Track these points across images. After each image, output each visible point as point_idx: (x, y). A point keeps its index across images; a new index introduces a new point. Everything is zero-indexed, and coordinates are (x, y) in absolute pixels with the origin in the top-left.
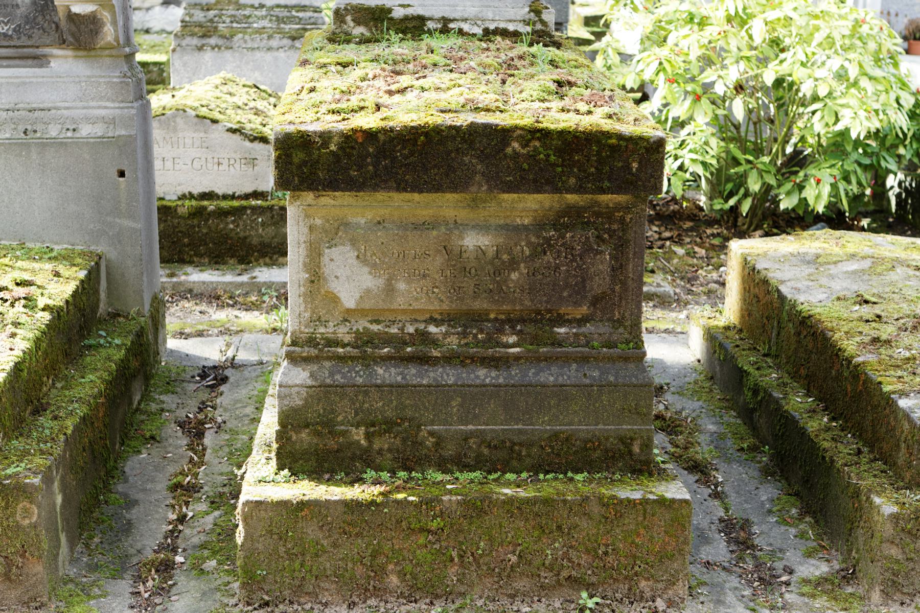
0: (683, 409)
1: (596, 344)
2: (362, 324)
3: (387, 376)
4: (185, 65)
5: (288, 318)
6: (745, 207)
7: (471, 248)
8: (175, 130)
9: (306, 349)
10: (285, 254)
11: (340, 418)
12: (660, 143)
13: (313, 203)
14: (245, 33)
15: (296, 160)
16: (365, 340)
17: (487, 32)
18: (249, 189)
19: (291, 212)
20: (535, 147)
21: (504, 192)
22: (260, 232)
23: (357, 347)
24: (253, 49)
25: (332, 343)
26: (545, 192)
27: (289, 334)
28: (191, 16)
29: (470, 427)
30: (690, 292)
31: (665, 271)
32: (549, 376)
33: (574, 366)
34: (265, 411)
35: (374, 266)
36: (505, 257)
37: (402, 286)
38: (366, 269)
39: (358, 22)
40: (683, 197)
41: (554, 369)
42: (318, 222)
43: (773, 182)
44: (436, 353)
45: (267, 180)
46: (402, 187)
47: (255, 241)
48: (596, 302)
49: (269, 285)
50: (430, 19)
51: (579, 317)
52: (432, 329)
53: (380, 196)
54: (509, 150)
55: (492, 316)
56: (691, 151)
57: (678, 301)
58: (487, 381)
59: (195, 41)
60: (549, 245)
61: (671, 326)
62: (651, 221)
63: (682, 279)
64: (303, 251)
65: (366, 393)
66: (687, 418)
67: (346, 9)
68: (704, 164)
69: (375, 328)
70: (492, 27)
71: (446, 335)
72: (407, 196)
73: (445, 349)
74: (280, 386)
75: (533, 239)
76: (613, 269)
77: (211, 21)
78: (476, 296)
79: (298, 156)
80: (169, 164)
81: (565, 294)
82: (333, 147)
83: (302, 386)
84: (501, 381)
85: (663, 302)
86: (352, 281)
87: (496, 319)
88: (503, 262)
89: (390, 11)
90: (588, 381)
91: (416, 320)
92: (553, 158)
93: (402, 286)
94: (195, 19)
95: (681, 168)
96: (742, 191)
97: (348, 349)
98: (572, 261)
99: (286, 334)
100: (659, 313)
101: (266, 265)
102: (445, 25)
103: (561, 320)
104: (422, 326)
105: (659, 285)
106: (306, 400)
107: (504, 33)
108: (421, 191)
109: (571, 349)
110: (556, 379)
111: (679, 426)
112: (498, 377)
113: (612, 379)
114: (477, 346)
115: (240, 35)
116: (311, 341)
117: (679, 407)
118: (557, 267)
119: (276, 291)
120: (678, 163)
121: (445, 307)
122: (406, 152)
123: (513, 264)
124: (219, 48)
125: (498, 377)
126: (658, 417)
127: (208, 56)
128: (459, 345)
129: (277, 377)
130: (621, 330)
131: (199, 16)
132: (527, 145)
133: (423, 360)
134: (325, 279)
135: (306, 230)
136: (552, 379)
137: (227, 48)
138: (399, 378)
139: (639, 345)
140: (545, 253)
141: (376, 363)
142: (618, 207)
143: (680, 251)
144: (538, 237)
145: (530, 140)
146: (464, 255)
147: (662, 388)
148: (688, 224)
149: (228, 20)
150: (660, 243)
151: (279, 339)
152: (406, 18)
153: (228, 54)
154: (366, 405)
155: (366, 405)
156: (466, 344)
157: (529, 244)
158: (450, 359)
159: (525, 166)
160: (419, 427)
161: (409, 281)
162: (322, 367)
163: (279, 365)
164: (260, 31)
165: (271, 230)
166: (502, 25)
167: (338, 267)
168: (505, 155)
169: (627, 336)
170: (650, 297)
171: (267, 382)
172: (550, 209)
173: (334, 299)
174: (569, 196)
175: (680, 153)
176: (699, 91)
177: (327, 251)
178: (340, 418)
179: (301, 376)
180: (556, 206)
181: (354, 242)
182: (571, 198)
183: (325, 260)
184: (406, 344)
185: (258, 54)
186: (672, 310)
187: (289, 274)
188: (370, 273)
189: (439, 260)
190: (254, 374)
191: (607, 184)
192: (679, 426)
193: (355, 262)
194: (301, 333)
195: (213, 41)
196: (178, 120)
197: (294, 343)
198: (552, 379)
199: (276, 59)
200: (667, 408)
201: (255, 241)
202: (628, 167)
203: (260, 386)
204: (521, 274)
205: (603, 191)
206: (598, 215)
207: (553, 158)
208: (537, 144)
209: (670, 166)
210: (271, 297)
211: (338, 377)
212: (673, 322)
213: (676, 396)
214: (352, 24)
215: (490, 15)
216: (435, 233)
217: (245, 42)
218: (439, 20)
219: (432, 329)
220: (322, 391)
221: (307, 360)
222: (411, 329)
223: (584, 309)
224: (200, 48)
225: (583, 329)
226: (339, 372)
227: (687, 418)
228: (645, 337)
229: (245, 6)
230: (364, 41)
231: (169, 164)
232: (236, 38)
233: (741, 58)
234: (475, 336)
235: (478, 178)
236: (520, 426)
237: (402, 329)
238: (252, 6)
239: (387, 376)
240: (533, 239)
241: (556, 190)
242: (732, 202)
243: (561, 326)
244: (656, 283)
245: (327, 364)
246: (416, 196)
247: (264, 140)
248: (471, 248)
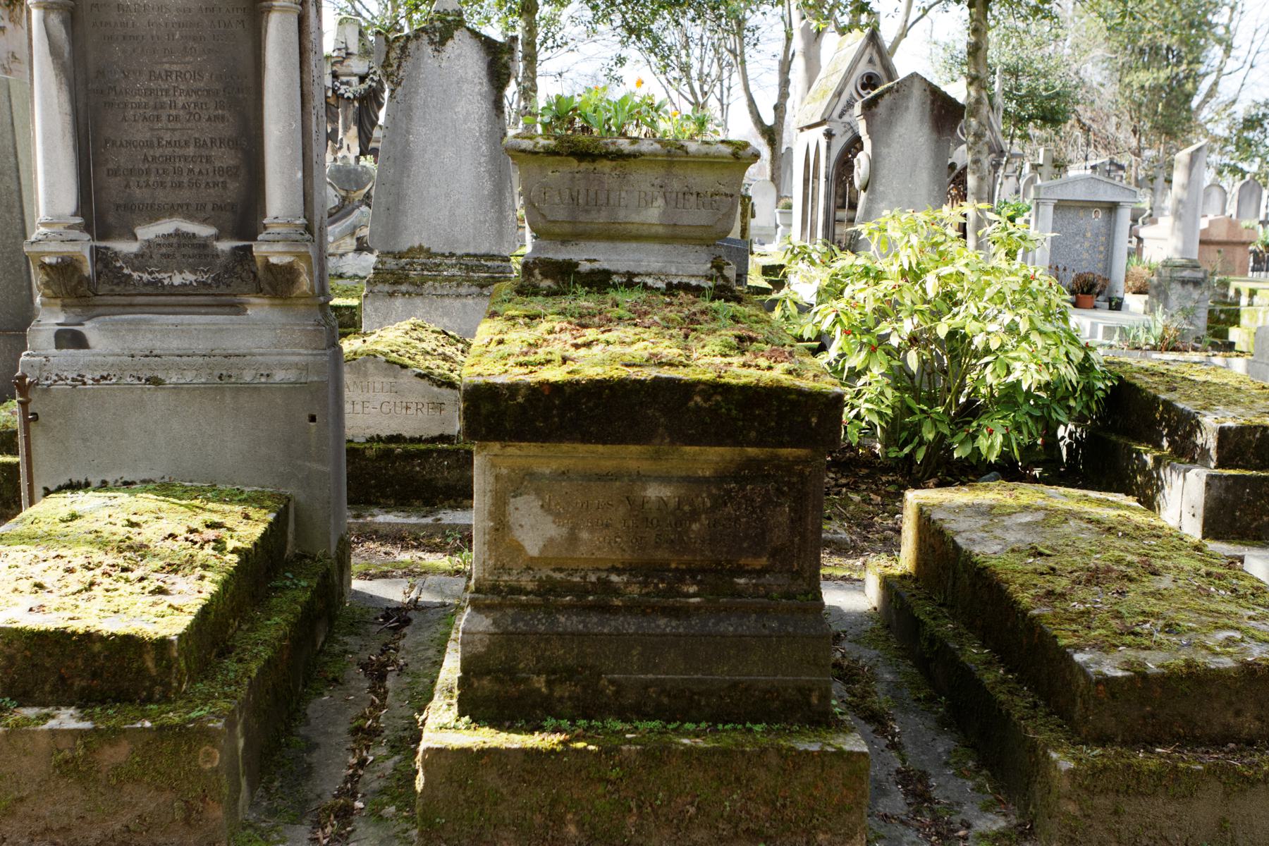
0: (860, 657)
1: (775, 595)
2: (545, 572)
3: (569, 623)
4: (376, 310)
5: (473, 561)
6: (920, 456)
7: (653, 498)
8: (366, 375)
9: (490, 596)
10: (472, 498)
11: (522, 665)
12: (839, 399)
13: (500, 453)
14: (435, 280)
15: (484, 411)
16: (548, 589)
17: (669, 285)
18: (436, 433)
19: (477, 461)
20: (717, 402)
21: (686, 445)
22: (446, 474)
23: (540, 595)
24: (442, 296)
25: (516, 590)
26: (726, 445)
27: (473, 581)
28: (383, 263)
29: (650, 676)
30: (866, 539)
31: (841, 517)
32: (728, 627)
33: (754, 616)
34: (447, 656)
35: (558, 515)
36: (687, 508)
37: (585, 535)
38: (550, 518)
39: (545, 275)
40: (859, 444)
41: (734, 619)
42: (504, 471)
43: (947, 431)
44: (617, 602)
45: (456, 426)
46: (586, 439)
47: (440, 484)
48: (774, 554)
49: (453, 527)
50: (616, 273)
51: (758, 567)
52: (614, 578)
53: (565, 447)
54: (692, 404)
55: (673, 566)
57: (854, 548)
58: (668, 630)
59: (387, 288)
60: (731, 498)
61: (847, 573)
62: (829, 466)
63: (858, 526)
64: (488, 500)
65: (548, 641)
66: (863, 667)
67: (534, 263)
69: (558, 576)
70: (675, 281)
71: (628, 583)
72: (591, 447)
73: (626, 598)
74: (463, 633)
75: (714, 491)
76: (792, 521)
77: (403, 268)
78: (657, 546)
79: (486, 408)
80: (358, 408)
81: (745, 545)
82: (520, 400)
83: (484, 633)
84: (681, 630)
85: (841, 549)
86: (535, 530)
87: (677, 569)
88: (685, 513)
89: (577, 265)
90: (767, 632)
91: (598, 569)
92: (734, 412)
93: (585, 535)
94: (387, 266)
95: (857, 416)
96: (916, 440)
97: (531, 596)
98: (752, 513)
99: (470, 578)
100: (836, 560)
101: (451, 507)
102: (630, 280)
103: (741, 572)
104: (604, 575)
105: (835, 532)
106: (488, 646)
107: (687, 288)
108: (604, 443)
109: (750, 600)
110: (736, 630)
111: (856, 674)
112: (678, 626)
113: (791, 630)
114: (658, 596)
115: (430, 283)
116: (495, 589)
117: (856, 655)
118: (737, 519)
119: (460, 533)
120: (854, 412)
121: (627, 556)
122: (591, 404)
123: (694, 515)
124: (410, 294)
125: (678, 626)
126: (836, 665)
127: (399, 302)
128: (640, 595)
129: (462, 621)
130: (800, 581)
131: (391, 263)
132: (709, 400)
133: (604, 609)
134: (510, 528)
135: (492, 479)
136: (731, 629)
137: (417, 295)
138: (581, 627)
139: (818, 596)
140: (726, 505)
141: (558, 611)
142: (798, 461)
143: (856, 498)
144: (719, 489)
145: (712, 395)
146: (646, 506)
147: (839, 635)
148: (864, 471)
149: (419, 268)
150: (836, 489)
151: (462, 582)
152: (592, 272)
153: (418, 301)
154: (548, 653)
155: (548, 653)
156: (647, 594)
157: (710, 495)
158: (630, 608)
159: (708, 420)
160: (599, 675)
161: (592, 531)
162: (505, 614)
163: (462, 608)
164: (449, 279)
165: (456, 474)
166: (685, 280)
167: (523, 516)
168: (688, 409)
169: (805, 587)
170: (828, 543)
171: (450, 625)
172: (732, 461)
173: (519, 548)
174: (749, 449)
175: (856, 402)
176: (874, 342)
177: (512, 500)
178: (522, 665)
179: (484, 623)
180: (737, 458)
181: (538, 492)
182: (752, 451)
183: (511, 508)
184: (589, 593)
185: (447, 301)
186: (849, 557)
187: (475, 517)
188: (554, 522)
189: (622, 510)
190: (436, 617)
191: (787, 438)
192: (856, 674)
193: (539, 511)
194: (485, 580)
195: (404, 288)
196: (369, 365)
197: (478, 590)
198: (731, 629)
199: (464, 306)
200: (843, 656)
201: (440, 484)
202: (808, 422)
203: (443, 630)
204: (702, 525)
205: (783, 445)
206: (778, 467)
207: (734, 412)
208: (719, 398)
209: (848, 415)
210: (455, 539)
211: (520, 624)
212: (850, 569)
213: (853, 645)
214: (540, 277)
215: (674, 270)
216: (618, 483)
217: (435, 289)
218: (623, 275)
219: (614, 578)
220: (504, 639)
221: (489, 608)
222: (593, 578)
223: (764, 561)
224: (391, 295)
225: (762, 580)
226: (522, 620)
227: (863, 667)
228: (823, 584)
229: (436, 255)
230: (551, 293)
231: (358, 408)
232: (426, 286)
233: (916, 311)
234: (656, 585)
235: (661, 430)
236: (700, 676)
237: (584, 578)
238: (443, 255)
239: (569, 623)
240: (714, 491)
241: (737, 443)
242: (906, 450)
243: (740, 577)
244: (835, 529)
245: (510, 611)
246: (600, 448)
247: (451, 385)
248: (653, 498)
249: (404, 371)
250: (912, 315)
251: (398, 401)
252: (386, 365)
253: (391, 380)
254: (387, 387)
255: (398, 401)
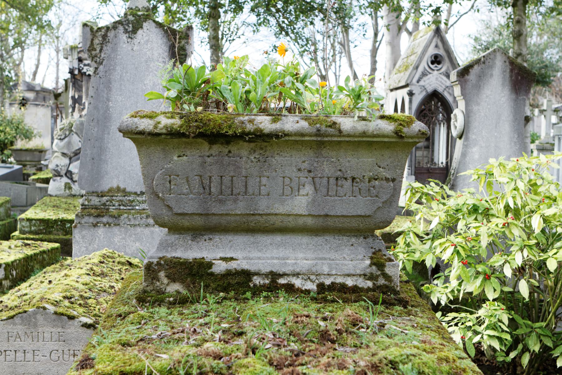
4: (83, 237)
6: (526, 360)
14: (129, 214)
24: (135, 225)
28: (89, 201)
43: (550, 344)
56: (487, 328)
59: (92, 220)
68: (500, 339)
77: (104, 204)
94: (92, 203)
96: (520, 346)
115: (126, 215)
124: (110, 225)
127: (101, 231)
131: (95, 201)
137: (115, 225)
149: (117, 204)
153: (116, 230)
164: (140, 212)
176: (489, 272)
185: (139, 230)
195: (105, 220)
199: (152, 233)
217: (129, 220)
224: (95, 225)
229: (130, 194)
232: (122, 218)
233: (525, 246)
238: (136, 193)
242: (512, 355)
249: (71, 322)
250: (522, 250)
251: (66, 350)
252: (54, 316)
253: (59, 330)
254: (55, 337)
255: (66, 350)
